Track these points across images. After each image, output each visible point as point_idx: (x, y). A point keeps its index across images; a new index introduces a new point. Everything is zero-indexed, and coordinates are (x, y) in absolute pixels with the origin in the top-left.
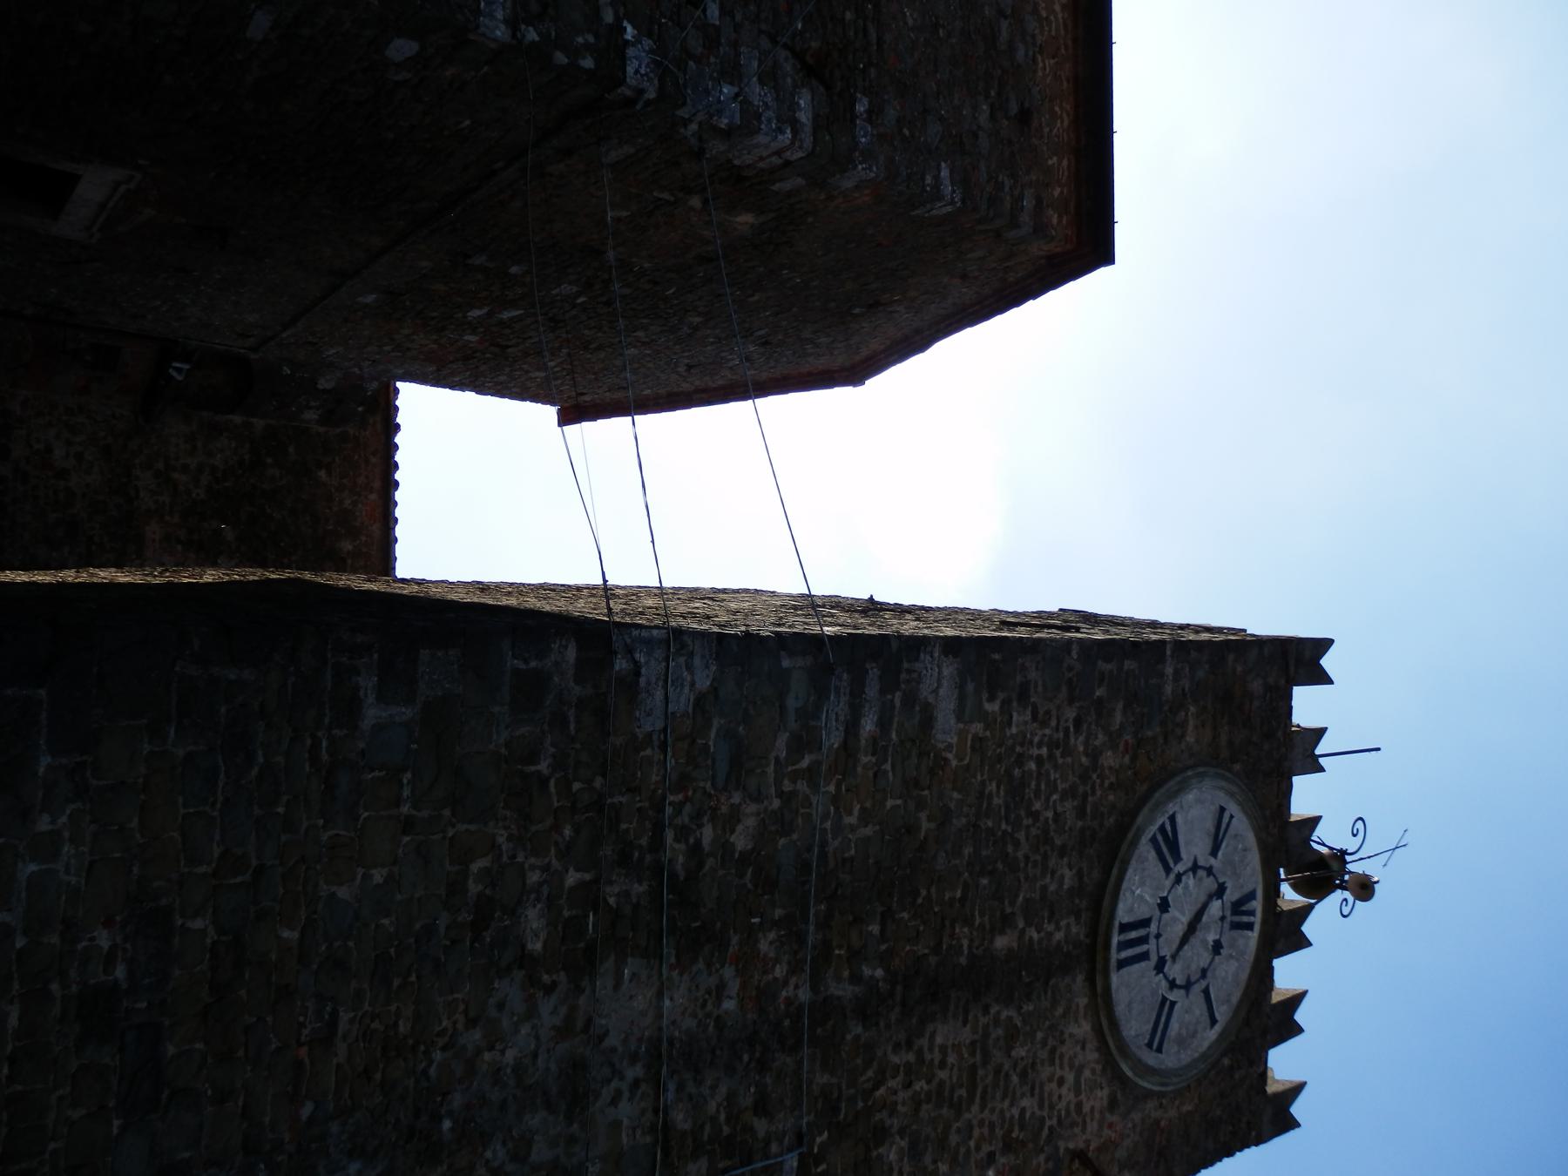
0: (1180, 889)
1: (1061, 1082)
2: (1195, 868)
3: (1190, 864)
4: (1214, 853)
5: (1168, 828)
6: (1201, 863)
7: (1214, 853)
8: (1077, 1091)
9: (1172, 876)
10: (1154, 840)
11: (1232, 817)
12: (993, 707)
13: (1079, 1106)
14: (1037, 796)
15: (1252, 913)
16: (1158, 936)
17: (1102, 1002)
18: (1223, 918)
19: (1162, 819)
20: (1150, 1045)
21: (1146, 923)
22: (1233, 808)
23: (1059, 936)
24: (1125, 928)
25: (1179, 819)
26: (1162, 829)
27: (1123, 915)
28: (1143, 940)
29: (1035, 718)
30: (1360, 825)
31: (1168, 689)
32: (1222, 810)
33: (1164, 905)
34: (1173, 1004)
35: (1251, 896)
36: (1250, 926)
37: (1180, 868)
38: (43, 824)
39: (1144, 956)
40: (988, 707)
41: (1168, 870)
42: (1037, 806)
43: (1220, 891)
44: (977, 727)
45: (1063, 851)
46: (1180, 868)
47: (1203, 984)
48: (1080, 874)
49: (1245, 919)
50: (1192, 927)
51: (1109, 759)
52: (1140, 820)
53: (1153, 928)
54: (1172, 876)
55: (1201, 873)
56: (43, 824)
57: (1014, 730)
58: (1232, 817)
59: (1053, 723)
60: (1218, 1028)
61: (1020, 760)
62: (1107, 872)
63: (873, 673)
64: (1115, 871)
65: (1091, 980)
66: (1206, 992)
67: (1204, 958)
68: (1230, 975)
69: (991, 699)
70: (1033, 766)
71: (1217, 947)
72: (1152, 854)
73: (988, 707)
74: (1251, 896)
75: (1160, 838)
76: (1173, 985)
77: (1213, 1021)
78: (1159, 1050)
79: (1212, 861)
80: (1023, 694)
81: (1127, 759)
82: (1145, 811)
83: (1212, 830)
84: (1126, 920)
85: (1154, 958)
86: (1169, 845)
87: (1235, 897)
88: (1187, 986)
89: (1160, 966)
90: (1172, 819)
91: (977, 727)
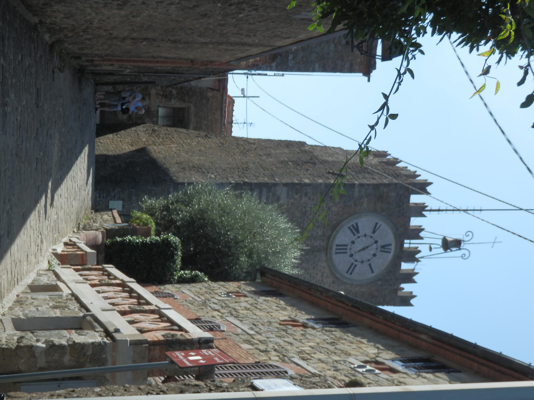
0: (359, 240)
1: (317, 274)
2: (365, 235)
3: (364, 234)
4: (374, 232)
5: (355, 226)
6: (367, 234)
7: (374, 232)
8: (322, 276)
9: (356, 237)
10: (349, 228)
11: (381, 225)
12: (297, 197)
13: (322, 281)
14: (310, 214)
15: (390, 249)
16: (350, 249)
17: (329, 260)
18: (377, 249)
19: (353, 223)
20: (347, 272)
21: (347, 245)
22: (380, 223)
23: (316, 244)
24: (337, 245)
25: (359, 224)
26: (353, 226)
27: (338, 241)
28: (346, 249)
29: (309, 199)
30: (470, 233)
31: (356, 194)
32: (377, 224)
33: (353, 242)
34: (356, 266)
35: (390, 245)
36: (389, 252)
37: (359, 235)
38: (133, 205)
39: (346, 253)
40: (295, 196)
41: (354, 235)
42: (310, 217)
43: (376, 242)
44: (292, 200)
45: (318, 227)
46: (359, 235)
47: (369, 263)
48: (324, 232)
49: (386, 250)
50: (364, 249)
51: (334, 209)
52: (343, 223)
53: (349, 247)
54: (356, 237)
55: (367, 237)
56: (133, 205)
57: (303, 201)
58: (381, 225)
59: (316, 200)
60: (373, 275)
61: (305, 207)
62: (332, 232)
63: (265, 190)
64: (334, 233)
65: (326, 254)
66: (370, 265)
67: (369, 257)
68: (382, 262)
69: (296, 194)
70: (309, 209)
71: (374, 255)
72: (349, 231)
73: (295, 196)
74: (390, 245)
75: (352, 228)
76: (356, 261)
77: (373, 272)
78: (351, 274)
79: (372, 235)
80: (306, 194)
81: (341, 209)
82: (345, 221)
83: (373, 227)
84: (339, 244)
85: (349, 254)
86: (355, 229)
87: (383, 244)
88: (362, 262)
89: (351, 256)
90: (357, 224)
91: (292, 200)
